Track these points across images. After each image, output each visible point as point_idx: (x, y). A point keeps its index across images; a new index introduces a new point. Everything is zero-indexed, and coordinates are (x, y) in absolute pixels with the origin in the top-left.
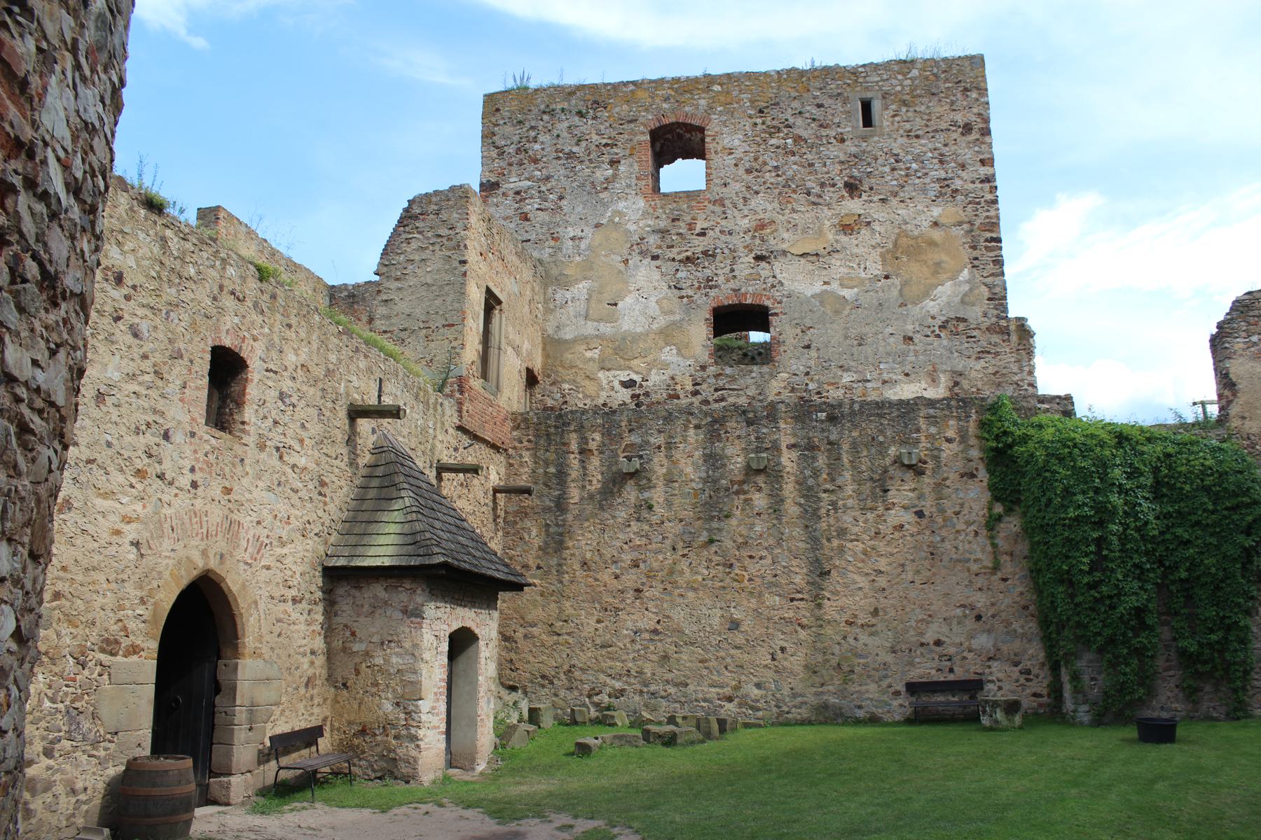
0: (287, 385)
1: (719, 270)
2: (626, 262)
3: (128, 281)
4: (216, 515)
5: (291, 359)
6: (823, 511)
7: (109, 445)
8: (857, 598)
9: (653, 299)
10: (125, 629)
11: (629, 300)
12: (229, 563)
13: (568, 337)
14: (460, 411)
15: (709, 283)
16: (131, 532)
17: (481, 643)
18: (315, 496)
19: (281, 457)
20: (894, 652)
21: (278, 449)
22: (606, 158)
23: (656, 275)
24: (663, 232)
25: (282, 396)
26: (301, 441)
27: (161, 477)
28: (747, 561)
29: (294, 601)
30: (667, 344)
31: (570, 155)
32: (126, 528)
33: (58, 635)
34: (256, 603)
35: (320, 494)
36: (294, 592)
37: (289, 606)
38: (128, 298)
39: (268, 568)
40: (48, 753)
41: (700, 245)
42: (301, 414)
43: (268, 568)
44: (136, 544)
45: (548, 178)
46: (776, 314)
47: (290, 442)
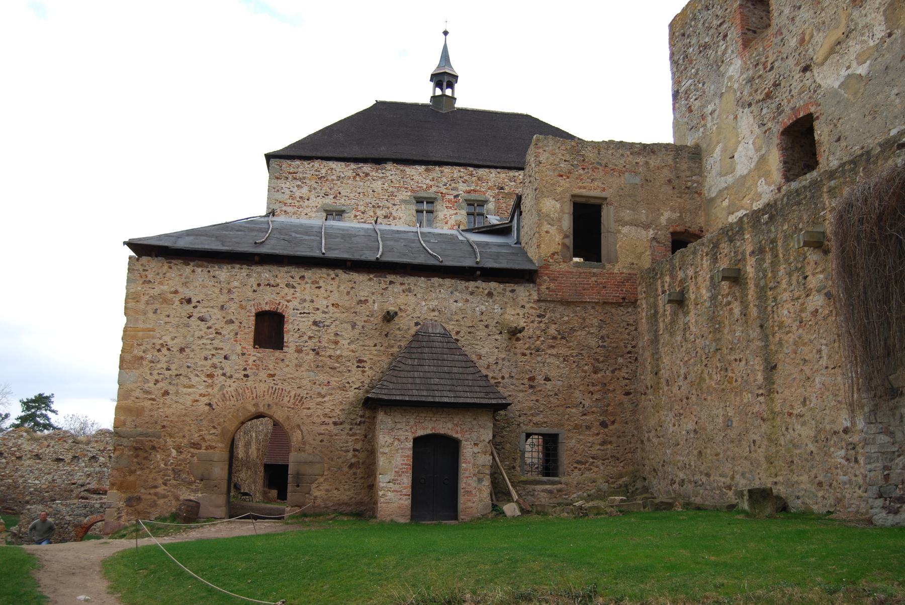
0: (319, 316)
1: (782, 96)
2: (736, 117)
3: (194, 300)
4: (262, 387)
5: (322, 303)
6: (769, 308)
7: (188, 367)
8: (793, 390)
9: (751, 142)
10: (204, 439)
11: (740, 148)
12: (274, 408)
13: (713, 195)
14: (539, 290)
15: (779, 110)
16: (205, 400)
17: (464, 443)
18: (354, 368)
19: (318, 354)
20: (817, 441)
21: (314, 350)
22: (721, 37)
23: (751, 119)
24: (750, 80)
25: (315, 323)
26: (336, 343)
27: (224, 375)
28: (734, 364)
29: (335, 424)
30: (760, 178)
31: (706, 46)
32: (202, 399)
33: (166, 442)
34: (299, 426)
35: (358, 367)
36: (334, 420)
37: (331, 427)
38: (195, 307)
39: (309, 409)
40: (165, 484)
41: (771, 77)
42: (333, 329)
43: (309, 409)
44: (210, 405)
45: (697, 73)
46: (818, 118)
47: (324, 344)
